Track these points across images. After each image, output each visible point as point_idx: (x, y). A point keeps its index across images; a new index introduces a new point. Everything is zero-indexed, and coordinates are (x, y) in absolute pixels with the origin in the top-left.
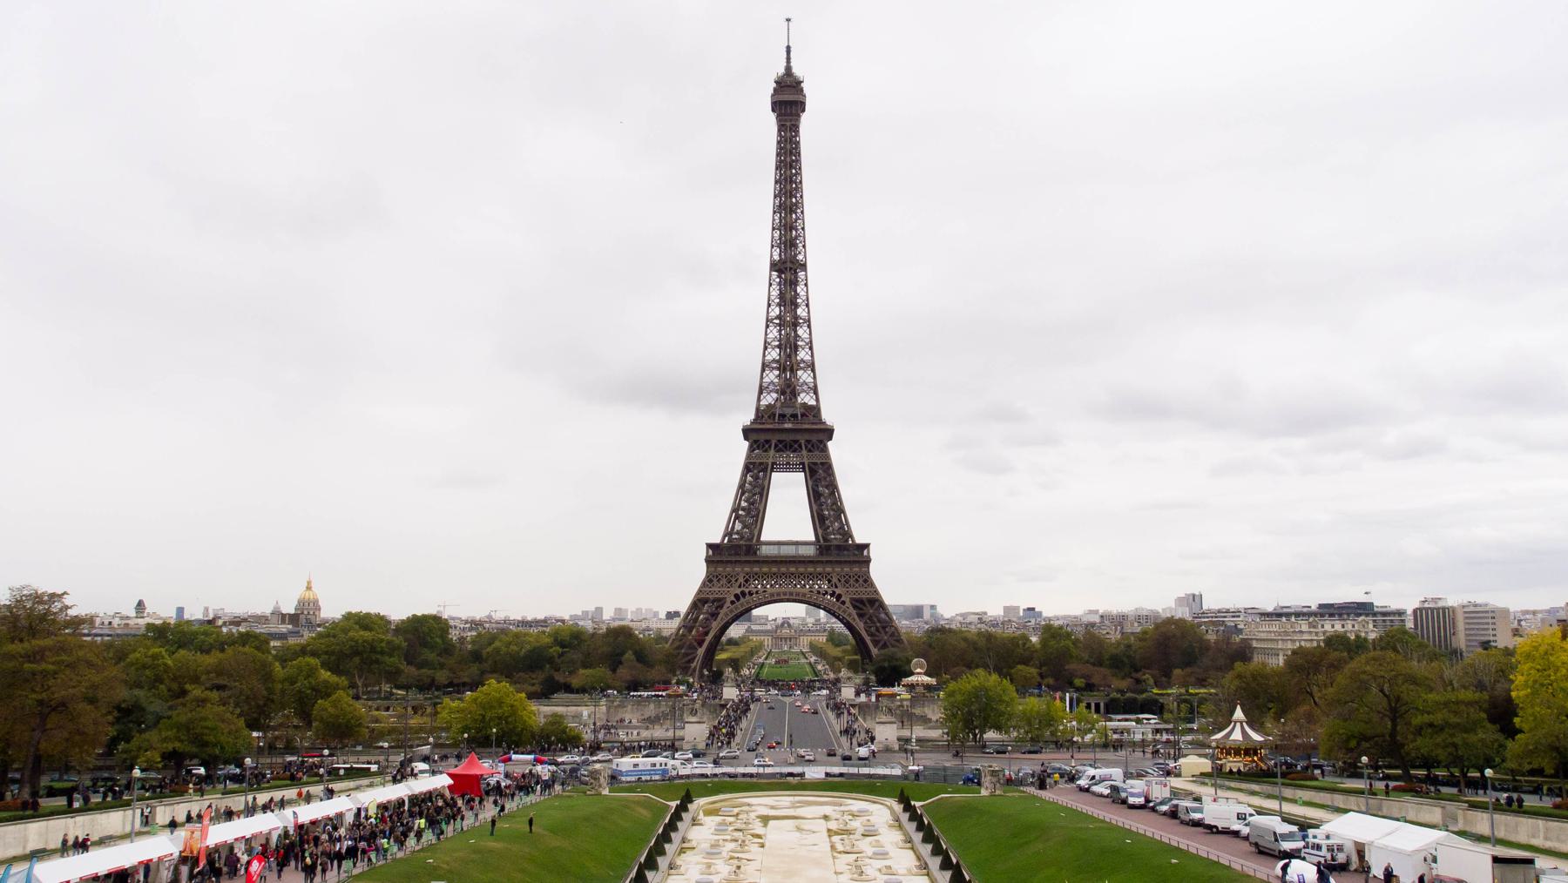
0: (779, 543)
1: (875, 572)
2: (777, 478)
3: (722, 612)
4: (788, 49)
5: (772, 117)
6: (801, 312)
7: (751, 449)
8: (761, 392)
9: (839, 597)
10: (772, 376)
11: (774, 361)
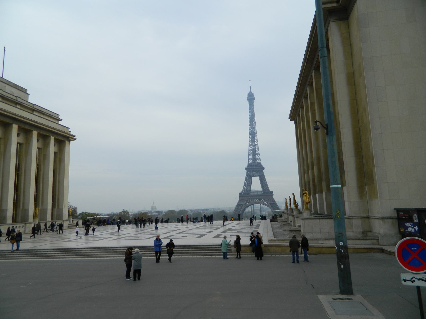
0: (254, 192)
1: (275, 197)
4: (250, 87)
5: (248, 102)
7: (247, 172)
8: (249, 160)
10: (251, 157)
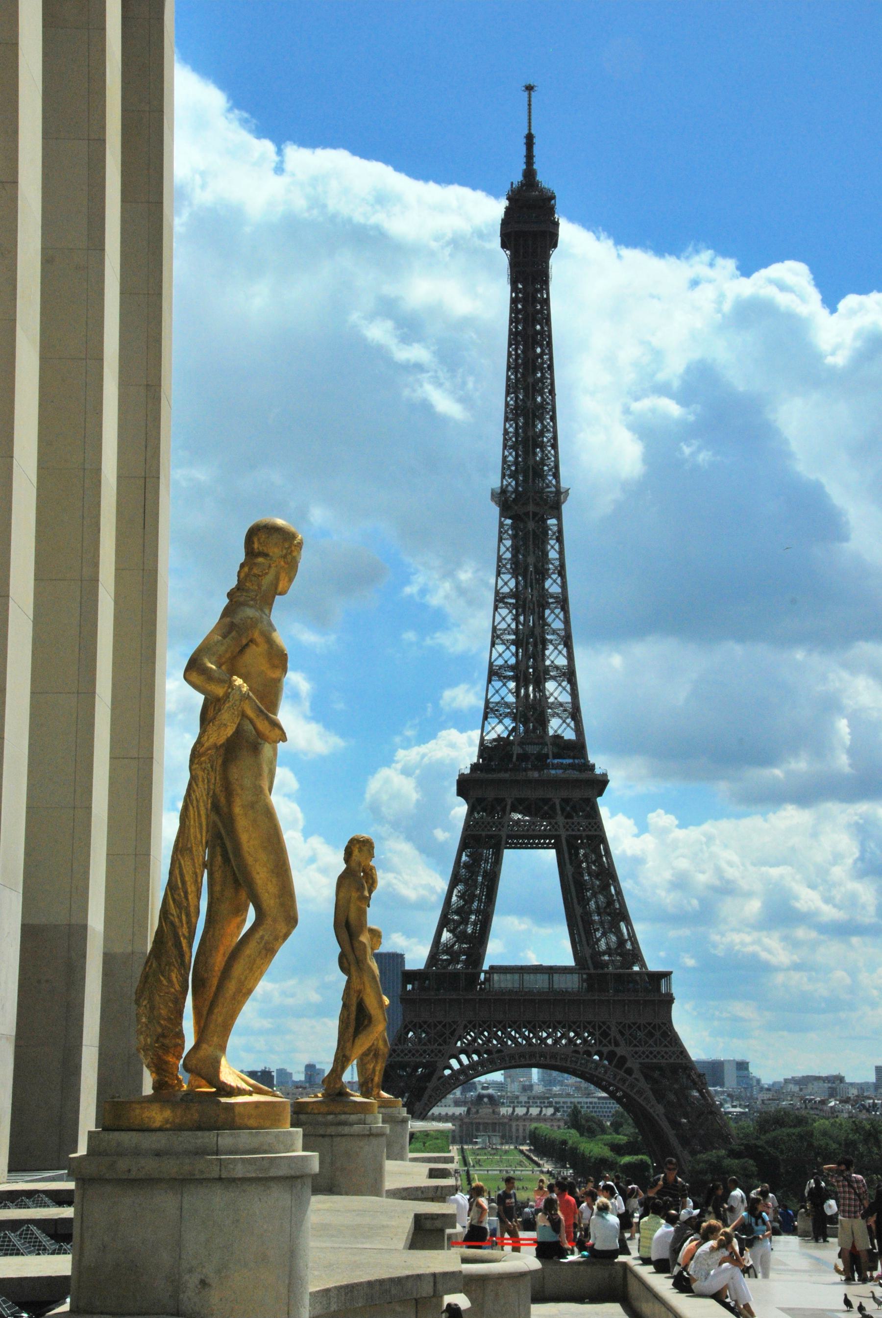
2: (510, 856)
3: (431, 1085)
4: (530, 140)
6: (552, 586)
7: (470, 813)
9: (623, 1060)
11: (506, 666)
